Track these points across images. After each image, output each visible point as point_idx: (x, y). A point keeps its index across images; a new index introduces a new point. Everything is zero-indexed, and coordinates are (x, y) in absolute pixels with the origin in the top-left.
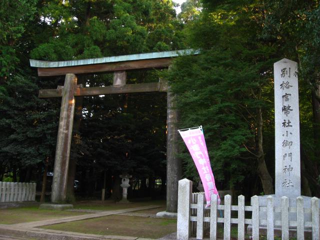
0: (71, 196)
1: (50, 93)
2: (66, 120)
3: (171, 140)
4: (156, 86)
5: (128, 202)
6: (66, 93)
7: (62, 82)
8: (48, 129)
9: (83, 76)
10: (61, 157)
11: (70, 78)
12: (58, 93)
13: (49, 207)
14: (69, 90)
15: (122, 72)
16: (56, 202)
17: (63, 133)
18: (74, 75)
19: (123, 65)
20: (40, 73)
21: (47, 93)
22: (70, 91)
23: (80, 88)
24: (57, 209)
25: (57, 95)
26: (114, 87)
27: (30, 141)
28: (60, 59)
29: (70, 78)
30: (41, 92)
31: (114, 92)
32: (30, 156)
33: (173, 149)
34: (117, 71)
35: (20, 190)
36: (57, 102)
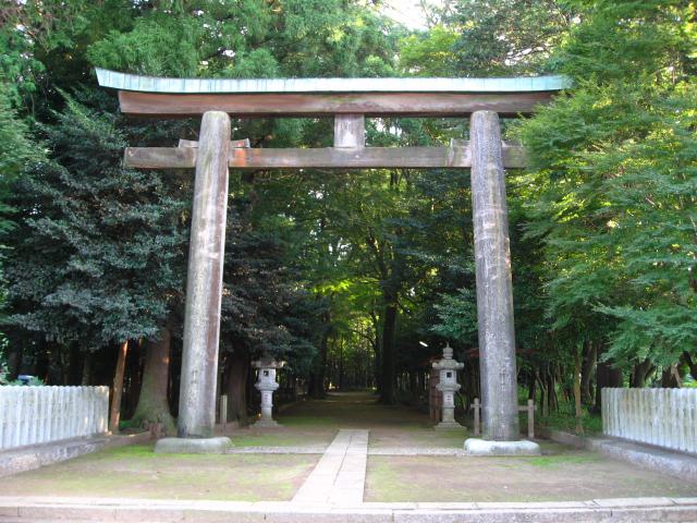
0: (164, 415)
1: (158, 157)
2: (214, 228)
3: (494, 278)
4: (444, 155)
5: (275, 424)
6: (210, 159)
7: (193, 134)
8: (166, 248)
9: (257, 125)
10: (206, 319)
11: (216, 122)
12: (181, 157)
13: (187, 446)
14: (217, 151)
15: (356, 118)
16: (199, 433)
17: (209, 259)
18: (227, 117)
19: (359, 101)
20: (125, 107)
21: (149, 157)
22: (221, 154)
23: (244, 147)
24: (210, 450)
25: (180, 164)
26: (337, 152)
27: (130, 280)
28: (170, 72)
29: (216, 122)
30: (130, 153)
31: (336, 162)
32: (127, 318)
33: (499, 299)
34: (344, 115)
35: (86, 409)
36: (181, 181)
